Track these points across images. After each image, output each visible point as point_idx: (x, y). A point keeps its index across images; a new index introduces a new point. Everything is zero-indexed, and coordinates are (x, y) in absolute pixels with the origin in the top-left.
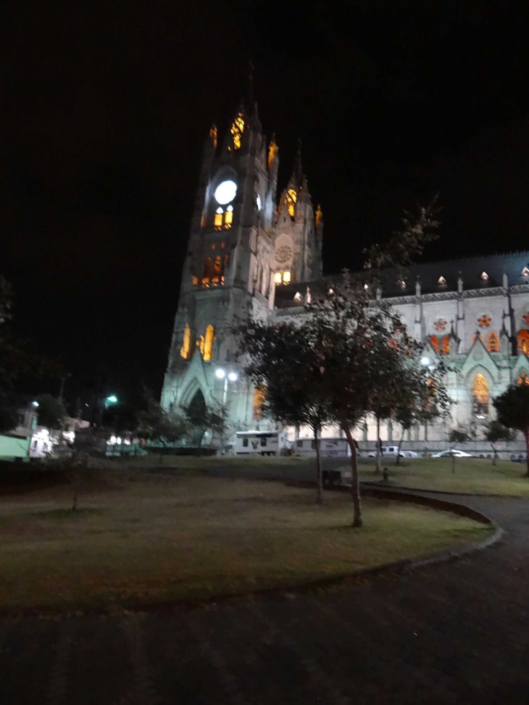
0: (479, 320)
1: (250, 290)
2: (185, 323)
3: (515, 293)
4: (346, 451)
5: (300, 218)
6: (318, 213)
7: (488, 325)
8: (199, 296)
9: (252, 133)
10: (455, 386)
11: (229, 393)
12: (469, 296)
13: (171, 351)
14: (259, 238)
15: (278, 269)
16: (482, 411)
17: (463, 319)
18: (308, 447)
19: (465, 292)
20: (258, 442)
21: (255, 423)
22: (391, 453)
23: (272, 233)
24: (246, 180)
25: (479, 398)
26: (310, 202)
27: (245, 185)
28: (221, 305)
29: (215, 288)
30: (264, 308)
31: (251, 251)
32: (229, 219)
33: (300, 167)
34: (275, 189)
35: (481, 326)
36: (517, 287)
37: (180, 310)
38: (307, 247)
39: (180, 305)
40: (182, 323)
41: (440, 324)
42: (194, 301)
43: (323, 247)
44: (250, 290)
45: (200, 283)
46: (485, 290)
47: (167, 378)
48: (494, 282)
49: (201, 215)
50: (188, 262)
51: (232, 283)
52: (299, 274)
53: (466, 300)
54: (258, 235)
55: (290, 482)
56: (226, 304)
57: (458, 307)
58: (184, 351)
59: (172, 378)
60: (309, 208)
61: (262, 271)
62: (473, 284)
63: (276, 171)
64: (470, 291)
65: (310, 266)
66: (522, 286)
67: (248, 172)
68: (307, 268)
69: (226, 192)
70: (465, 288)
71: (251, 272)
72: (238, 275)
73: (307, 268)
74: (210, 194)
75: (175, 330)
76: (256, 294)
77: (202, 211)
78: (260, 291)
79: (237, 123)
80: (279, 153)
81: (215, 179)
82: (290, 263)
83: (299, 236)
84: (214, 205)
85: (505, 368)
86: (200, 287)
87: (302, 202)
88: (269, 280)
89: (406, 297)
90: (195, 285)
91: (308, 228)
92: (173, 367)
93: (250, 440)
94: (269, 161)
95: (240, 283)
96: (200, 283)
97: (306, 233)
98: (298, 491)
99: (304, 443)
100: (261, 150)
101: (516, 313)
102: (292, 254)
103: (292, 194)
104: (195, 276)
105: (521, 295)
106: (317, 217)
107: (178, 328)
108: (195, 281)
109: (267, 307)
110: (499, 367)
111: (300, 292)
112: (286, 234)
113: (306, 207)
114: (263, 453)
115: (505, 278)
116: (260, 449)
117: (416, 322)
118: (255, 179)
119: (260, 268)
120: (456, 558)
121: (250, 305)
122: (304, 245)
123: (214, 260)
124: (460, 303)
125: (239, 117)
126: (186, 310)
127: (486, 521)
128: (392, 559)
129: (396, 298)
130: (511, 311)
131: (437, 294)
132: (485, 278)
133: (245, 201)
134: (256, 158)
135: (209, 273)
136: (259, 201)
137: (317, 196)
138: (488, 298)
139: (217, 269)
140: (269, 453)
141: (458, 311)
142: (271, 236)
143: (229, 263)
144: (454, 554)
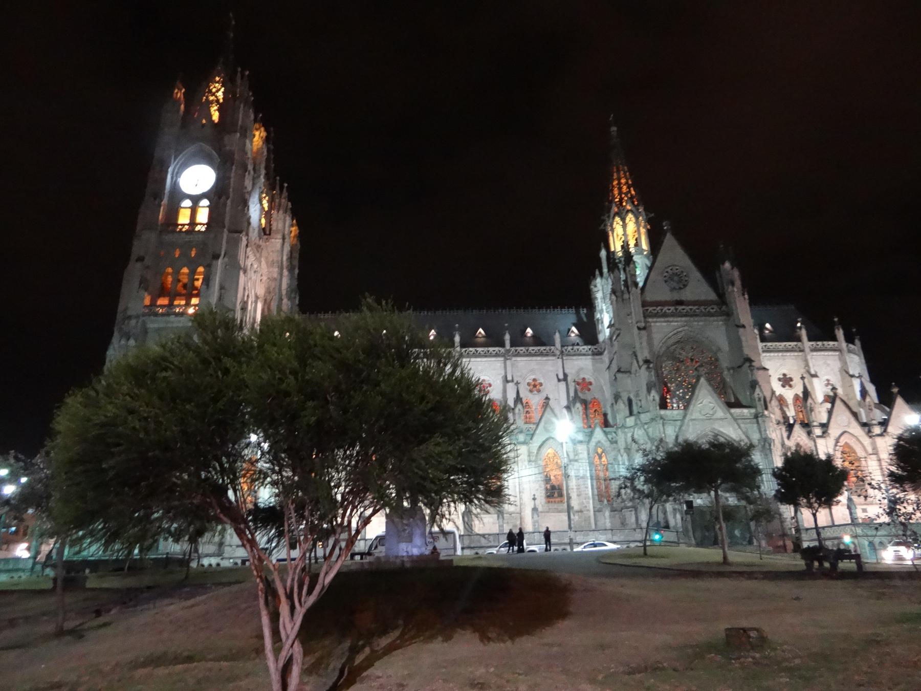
0: (529, 384)
3: (567, 355)
4: (455, 548)
5: (277, 231)
6: (293, 229)
7: (539, 391)
9: (242, 106)
10: (526, 463)
12: (518, 355)
14: (249, 249)
16: (556, 495)
17: (512, 381)
19: (513, 349)
26: (289, 212)
32: (203, 216)
35: (531, 391)
36: (570, 348)
39: (116, 334)
42: (145, 331)
43: (299, 274)
45: (153, 304)
48: (542, 340)
49: (160, 206)
50: (134, 271)
53: (514, 359)
60: (288, 219)
62: (518, 341)
63: (263, 165)
64: (519, 349)
65: (289, 299)
66: (576, 347)
67: (236, 157)
68: (285, 301)
69: (197, 178)
72: (220, 298)
73: (285, 301)
74: (172, 178)
79: (214, 90)
83: (275, 257)
84: (177, 195)
87: (281, 212)
91: (287, 248)
96: (153, 304)
101: (569, 379)
102: (264, 278)
104: (149, 294)
105: (575, 358)
108: (147, 301)
113: (285, 217)
115: (557, 337)
117: (559, 380)
118: (246, 170)
124: (508, 362)
125: (218, 82)
130: (565, 375)
131: (480, 349)
132: (529, 335)
133: (231, 195)
135: (163, 291)
141: (506, 373)
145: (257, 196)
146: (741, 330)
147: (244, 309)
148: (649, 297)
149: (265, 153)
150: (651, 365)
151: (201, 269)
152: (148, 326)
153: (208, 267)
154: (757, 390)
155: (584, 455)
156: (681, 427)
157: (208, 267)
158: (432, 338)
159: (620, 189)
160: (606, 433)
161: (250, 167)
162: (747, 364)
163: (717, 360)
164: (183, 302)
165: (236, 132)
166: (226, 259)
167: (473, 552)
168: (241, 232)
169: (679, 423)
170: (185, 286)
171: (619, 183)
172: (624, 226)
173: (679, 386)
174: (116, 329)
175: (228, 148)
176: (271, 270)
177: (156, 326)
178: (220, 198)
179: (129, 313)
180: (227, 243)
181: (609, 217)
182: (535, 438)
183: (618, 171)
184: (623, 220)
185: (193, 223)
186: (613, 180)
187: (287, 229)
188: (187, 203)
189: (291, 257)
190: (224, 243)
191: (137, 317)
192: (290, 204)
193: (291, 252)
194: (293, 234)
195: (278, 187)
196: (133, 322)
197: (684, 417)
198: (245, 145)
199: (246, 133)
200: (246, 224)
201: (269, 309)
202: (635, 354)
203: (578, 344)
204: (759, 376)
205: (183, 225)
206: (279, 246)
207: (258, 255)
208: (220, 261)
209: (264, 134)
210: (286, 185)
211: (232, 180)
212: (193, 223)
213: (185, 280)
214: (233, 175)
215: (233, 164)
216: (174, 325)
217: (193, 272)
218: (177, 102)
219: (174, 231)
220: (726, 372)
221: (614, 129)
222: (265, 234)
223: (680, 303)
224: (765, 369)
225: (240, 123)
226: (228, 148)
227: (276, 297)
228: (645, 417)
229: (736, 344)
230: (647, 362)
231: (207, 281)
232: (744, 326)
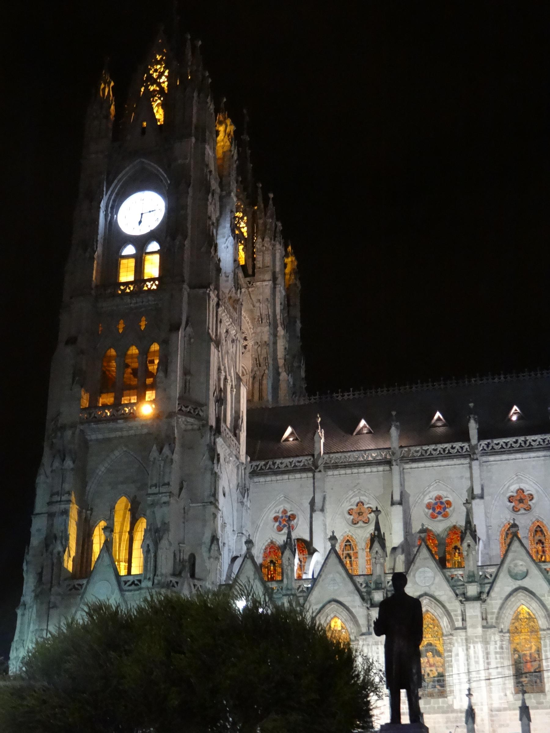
2: (69, 493)
6: (288, 260)
9: (195, 95)
14: (220, 309)
23: (237, 301)
24: (190, 190)
28: (154, 453)
31: (211, 339)
32: (152, 267)
37: (49, 465)
38: (281, 331)
39: (47, 452)
42: (85, 444)
43: (302, 329)
50: (65, 357)
52: (268, 384)
56: (166, 450)
58: (69, 556)
61: (226, 379)
65: (290, 370)
68: (284, 375)
69: (141, 212)
72: (186, 388)
73: (284, 375)
74: (106, 216)
76: (222, 429)
78: (225, 421)
79: (155, 75)
81: (116, 185)
83: (264, 309)
84: (117, 239)
86: (92, 414)
87: (267, 239)
89: (530, 438)
91: (281, 292)
95: (191, 405)
97: (278, 302)
102: (250, 343)
104: (87, 391)
106: (288, 270)
107: (50, 503)
111: (293, 427)
113: (274, 245)
118: (208, 190)
121: (214, 456)
122: (275, 327)
125: (159, 63)
126: (69, 463)
129: (511, 440)
134: (207, 147)
135: (106, 384)
143: (165, 365)
145: (228, 225)
147: (221, 401)
151: (155, 347)
152: (88, 438)
157: (165, 343)
158: (514, 418)
161: (214, 185)
164: (134, 400)
165: (190, 135)
168: (207, 286)
170: (135, 372)
174: (45, 444)
175: (180, 161)
176: (259, 330)
177: (100, 436)
178: (174, 238)
179: (63, 420)
180: (189, 304)
187: (278, 263)
188: (130, 250)
189: (288, 305)
190: (185, 306)
191: (73, 426)
192: (279, 224)
193: (288, 297)
194: (288, 270)
195: (260, 199)
196: (69, 433)
198: (203, 154)
199: (206, 135)
200: (213, 273)
201: (260, 391)
205: (127, 284)
206: (268, 291)
207: (236, 316)
209: (231, 128)
210: (271, 196)
211: (189, 211)
213: (135, 365)
214: (189, 201)
216: (125, 433)
217: (145, 352)
218: (105, 102)
219: (114, 295)
222: (246, 275)
225: (194, 120)
226: (180, 161)
227: (269, 373)
231: (165, 365)
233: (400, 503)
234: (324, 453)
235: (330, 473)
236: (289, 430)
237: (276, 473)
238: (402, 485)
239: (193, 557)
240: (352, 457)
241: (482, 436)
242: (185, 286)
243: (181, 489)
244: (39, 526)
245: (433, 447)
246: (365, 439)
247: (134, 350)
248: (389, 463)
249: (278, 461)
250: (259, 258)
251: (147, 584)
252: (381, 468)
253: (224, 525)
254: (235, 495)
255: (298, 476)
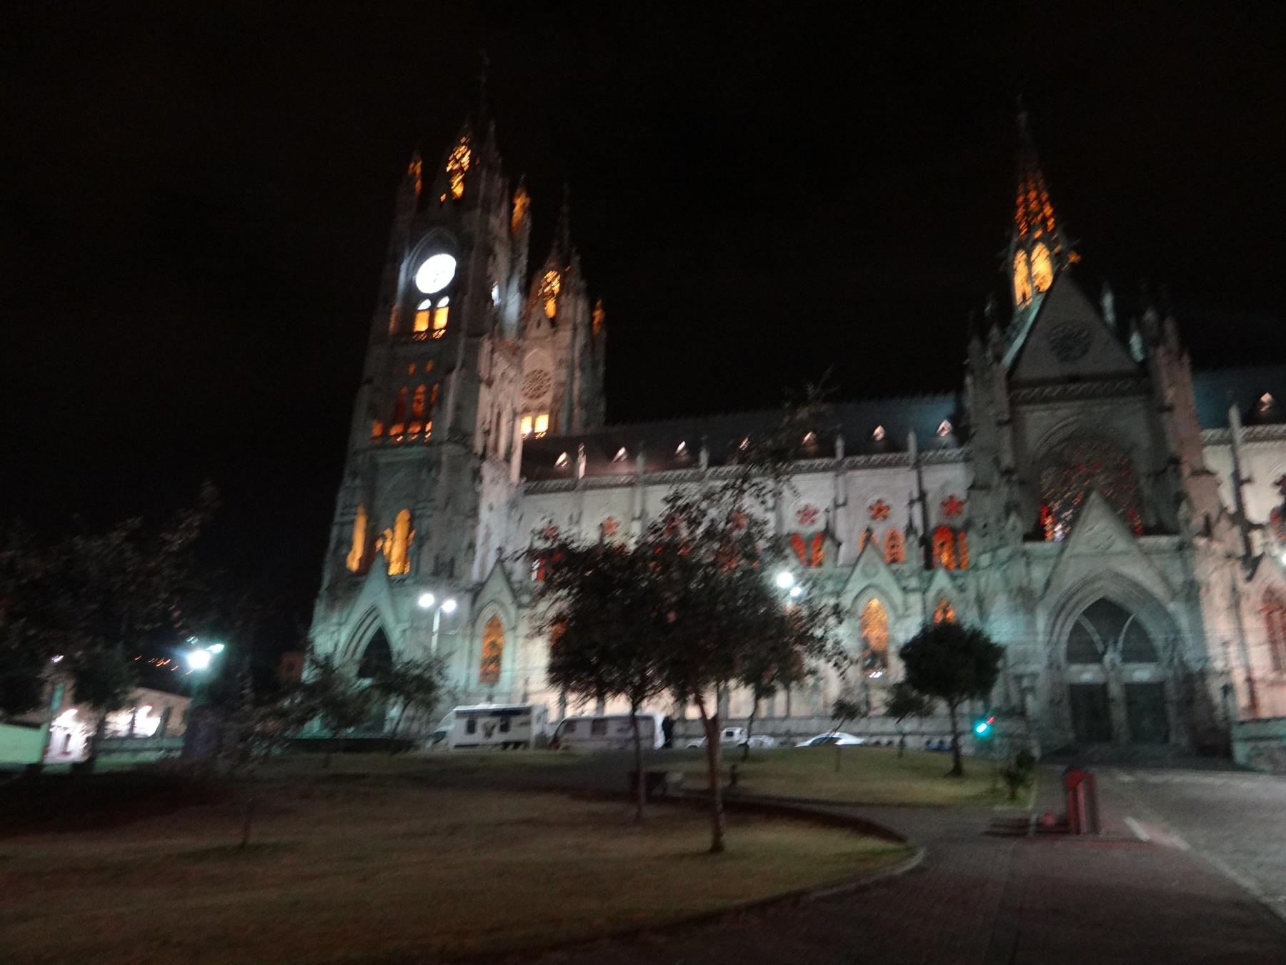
0: (871, 508)
1: (479, 448)
6: (598, 314)
8: (384, 458)
9: (484, 173)
11: (442, 634)
12: (854, 467)
13: (329, 556)
14: (496, 355)
15: (526, 411)
17: (844, 504)
18: (584, 731)
20: (493, 727)
21: (486, 690)
22: (728, 740)
23: (519, 348)
24: (473, 252)
25: (873, 643)
27: (472, 262)
29: (412, 444)
30: (502, 481)
32: (441, 319)
33: (567, 233)
34: (524, 270)
37: (347, 481)
38: (578, 374)
39: (347, 472)
40: (350, 507)
41: (807, 514)
42: (374, 466)
43: (607, 373)
44: (479, 448)
45: (385, 433)
46: (882, 457)
47: (320, 609)
48: (894, 444)
49: (390, 313)
50: (365, 393)
51: (445, 435)
52: (563, 417)
53: (849, 474)
54: (493, 352)
55: (577, 792)
56: (433, 473)
57: (836, 487)
59: (331, 607)
60: (582, 305)
61: (499, 414)
62: (860, 447)
63: (525, 241)
65: (585, 406)
66: (940, 452)
69: (435, 272)
70: (847, 453)
71: (480, 416)
74: (407, 275)
75: (337, 519)
77: (391, 307)
78: (496, 449)
80: (531, 210)
82: (547, 399)
83: (563, 354)
84: (414, 296)
85: (914, 590)
88: (512, 431)
90: (375, 438)
91: (581, 340)
92: (331, 588)
93: (481, 722)
94: (514, 224)
95: (461, 435)
96: (385, 433)
98: (596, 807)
99: (578, 726)
100: (500, 205)
101: (929, 498)
103: (553, 282)
107: (342, 514)
108: (377, 430)
109: (508, 477)
110: (905, 590)
112: (543, 347)
114: (506, 745)
115: (912, 440)
116: (498, 737)
118: (489, 252)
119: (496, 411)
120: (863, 889)
121: (477, 475)
123: (413, 393)
124: (840, 479)
127: (900, 839)
128: (781, 889)
135: (401, 414)
136: (495, 293)
137: (595, 282)
138: (885, 471)
139: (419, 408)
140: (517, 744)
142: (516, 353)
143: (441, 400)
144: (863, 882)
146: (1165, 416)
148: (1025, 373)
149: (529, 224)
150: (1014, 478)
153: (442, 382)
154: (1184, 508)
155: (917, 608)
156: (1055, 567)
159: (1027, 207)
160: (953, 578)
162: (1172, 467)
163: (1130, 462)
166: (464, 371)
167: (925, 739)
168: (481, 335)
169: (1052, 562)
171: (1026, 201)
172: (1029, 263)
173: (1066, 507)
181: (1008, 251)
182: (849, 587)
183: (1025, 181)
184: (1029, 254)
185: (431, 329)
186: (1017, 197)
191: (365, 451)
196: (360, 458)
197: (1062, 551)
201: (556, 421)
202: (997, 462)
203: (945, 447)
204: (1194, 487)
205: (420, 333)
207: (515, 360)
208: (454, 375)
209: (528, 200)
212: (431, 329)
215: (471, 249)
220: (1143, 481)
221: (1023, 117)
223: (1075, 379)
224: (1209, 473)
228: (1003, 553)
229: (1158, 435)
230: (1008, 472)
232: (1170, 409)
233: (639, 518)
234: (586, 475)
235: (588, 493)
236: (563, 457)
237: (545, 491)
238: (644, 503)
239: (452, 561)
240: (606, 479)
241: (710, 465)
242: (461, 335)
243: (447, 504)
244: (335, 532)
245: (669, 473)
246: (623, 463)
247: (421, 389)
248: (630, 484)
249: (548, 482)
250: (563, 312)
251: (408, 581)
252: (629, 489)
253: (488, 535)
254: (505, 510)
255: (563, 495)
